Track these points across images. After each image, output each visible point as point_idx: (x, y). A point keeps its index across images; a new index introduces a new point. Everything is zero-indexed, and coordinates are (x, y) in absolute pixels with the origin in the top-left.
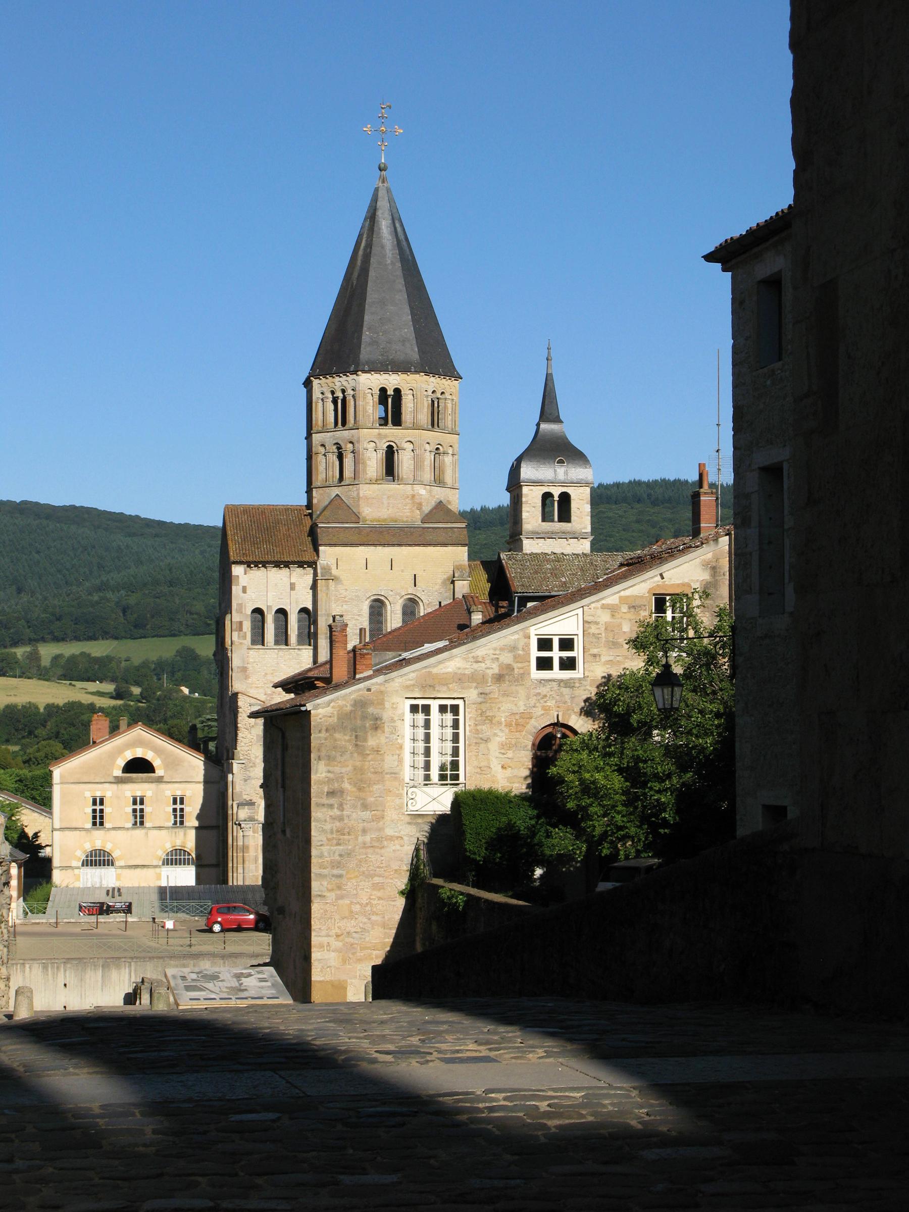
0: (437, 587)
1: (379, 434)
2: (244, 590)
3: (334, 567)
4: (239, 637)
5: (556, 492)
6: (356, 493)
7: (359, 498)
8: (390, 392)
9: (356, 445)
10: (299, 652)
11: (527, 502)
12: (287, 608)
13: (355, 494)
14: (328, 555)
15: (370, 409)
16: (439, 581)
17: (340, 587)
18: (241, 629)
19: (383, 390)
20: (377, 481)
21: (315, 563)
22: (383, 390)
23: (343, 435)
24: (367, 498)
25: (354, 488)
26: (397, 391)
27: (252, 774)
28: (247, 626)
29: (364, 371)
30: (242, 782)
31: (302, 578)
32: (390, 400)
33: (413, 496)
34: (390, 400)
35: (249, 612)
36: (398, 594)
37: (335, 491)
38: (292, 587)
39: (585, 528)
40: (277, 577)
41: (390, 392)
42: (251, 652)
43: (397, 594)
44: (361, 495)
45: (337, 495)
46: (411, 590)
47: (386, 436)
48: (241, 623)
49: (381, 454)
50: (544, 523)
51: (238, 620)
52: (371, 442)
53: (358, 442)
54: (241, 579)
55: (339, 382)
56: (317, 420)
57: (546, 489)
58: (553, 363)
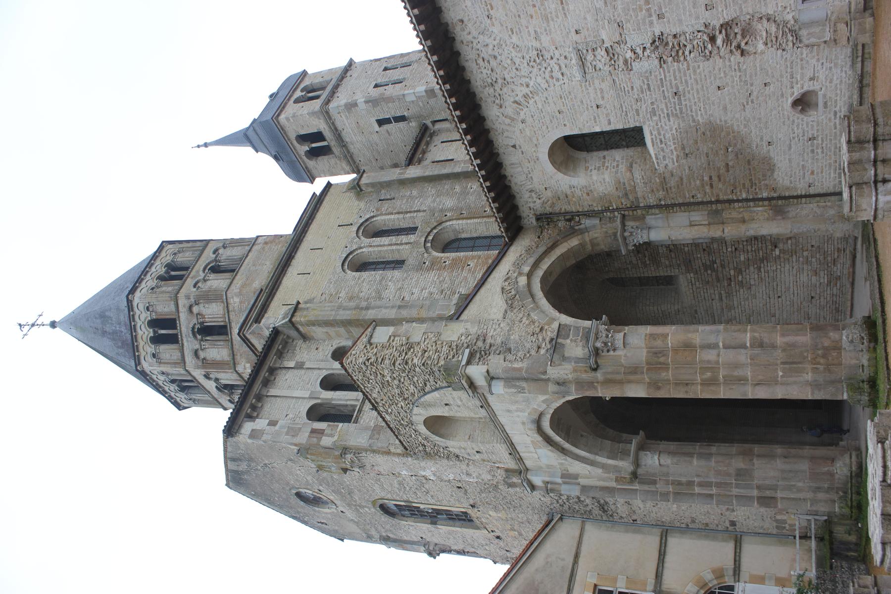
4: (332, 436)
12: (325, 373)
13: (237, 300)
18: (321, 432)
19: (161, 278)
25: (231, 301)
27: (499, 340)
28: (322, 425)
30: (510, 357)
32: (173, 273)
36: (354, 239)
38: (300, 366)
43: (352, 242)
46: (355, 228)
48: (313, 431)
49: (212, 276)
51: (307, 434)
58: (208, 141)
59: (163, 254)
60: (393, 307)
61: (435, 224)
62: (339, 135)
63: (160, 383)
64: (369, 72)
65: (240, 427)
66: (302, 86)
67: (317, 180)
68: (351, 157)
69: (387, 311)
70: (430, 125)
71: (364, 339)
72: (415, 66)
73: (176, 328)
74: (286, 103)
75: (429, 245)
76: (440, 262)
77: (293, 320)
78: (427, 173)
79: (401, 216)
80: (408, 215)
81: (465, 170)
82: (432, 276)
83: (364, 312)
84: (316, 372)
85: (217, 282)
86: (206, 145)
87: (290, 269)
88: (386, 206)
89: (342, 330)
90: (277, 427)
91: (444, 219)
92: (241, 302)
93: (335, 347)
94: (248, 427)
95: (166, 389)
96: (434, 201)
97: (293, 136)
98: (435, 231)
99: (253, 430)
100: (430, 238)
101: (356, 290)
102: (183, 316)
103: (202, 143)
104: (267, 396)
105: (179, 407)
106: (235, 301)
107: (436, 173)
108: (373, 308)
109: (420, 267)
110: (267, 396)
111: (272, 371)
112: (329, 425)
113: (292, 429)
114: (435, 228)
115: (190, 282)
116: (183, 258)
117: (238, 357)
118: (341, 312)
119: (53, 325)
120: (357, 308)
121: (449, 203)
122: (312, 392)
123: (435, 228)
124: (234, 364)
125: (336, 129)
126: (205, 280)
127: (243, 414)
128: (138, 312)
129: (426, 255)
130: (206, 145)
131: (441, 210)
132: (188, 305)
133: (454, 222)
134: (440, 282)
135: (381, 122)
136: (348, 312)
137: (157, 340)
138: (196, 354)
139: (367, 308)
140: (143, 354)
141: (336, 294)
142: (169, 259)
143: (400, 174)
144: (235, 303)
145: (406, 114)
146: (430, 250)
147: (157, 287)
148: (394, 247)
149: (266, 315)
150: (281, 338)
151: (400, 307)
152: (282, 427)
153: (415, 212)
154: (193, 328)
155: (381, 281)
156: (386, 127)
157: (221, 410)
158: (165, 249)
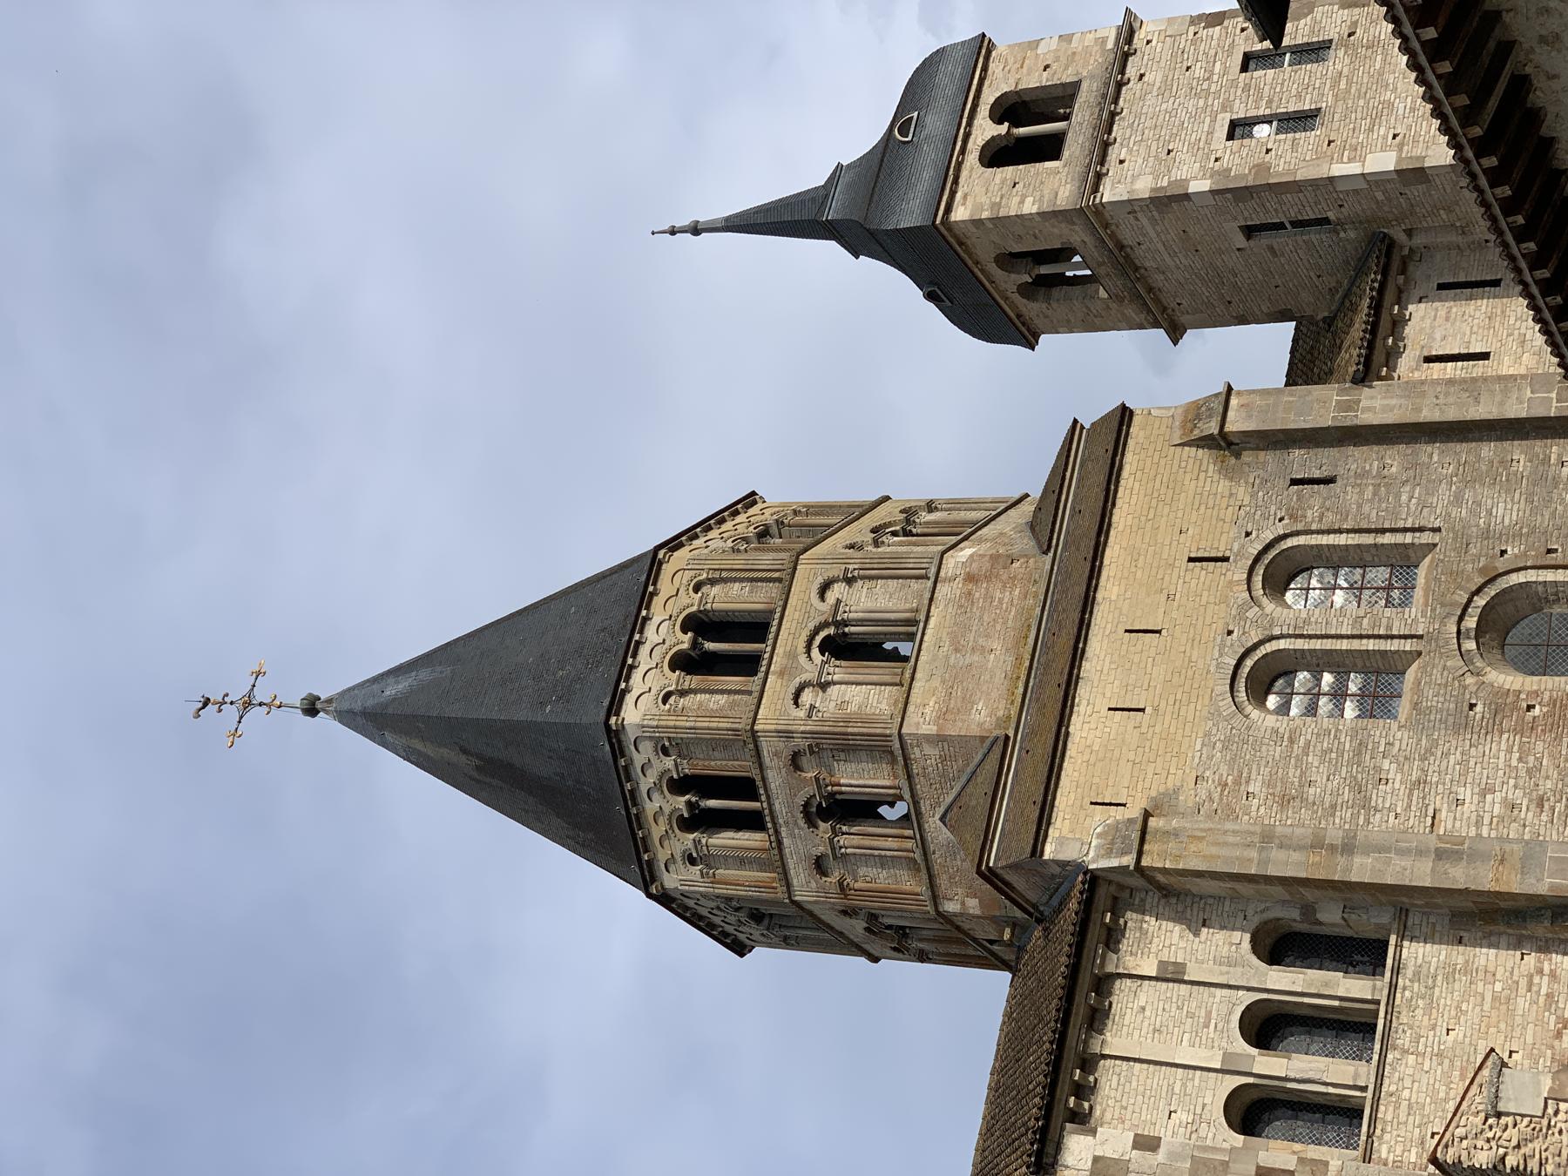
0: (1242, 493)
1: (781, 674)
2: (1147, 1143)
3: (1118, 814)
5: (985, 130)
6: (929, 750)
7: (939, 739)
8: (685, 641)
9: (803, 744)
10: (1409, 973)
11: (996, 206)
13: (932, 751)
14: (1079, 836)
15: (713, 705)
16: (1224, 485)
17: (1187, 799)
19: (681, 662)
20: (907, 687)
21: (1094, 879)
22: (681, 662)
23: (783, 793)
24: (943, 715)
25: (916, 753)
26: (698, 624)
29: (615, 705)
31: (1152, 941)
32: (710, 646)
33: (971, 578)
34: (710, 646)
35: (1239, 1140)
36: (1243, 609)
37: (933, 823)
38: (1171, 975)
39: (1104, 40)
40: (1138, 1022)
41: (685, 641)
42: (1382, 1151)
43: (1241, 616)
44: (932, 729)
45: (942, 819)
47: (792, 655)
49: (838, 670)
50: (1066, 154)
52: (795, 695)
53: (787, 734)
54: (1108, 1152)
55: (660, 806)
56: (757, 885)
57: (972, 158)
58: (703, 217)
59: (665, 586)
60: (1420, 853)
61: (1480, 580)
62: (1127, 257)
63: (704, 912)
64: (1198, 71)
65: (1058, 1147)
66: (989, 97)
67: (1044, 339)
68: (1157, 301)
69: (1406, 862)
70: (1400, 237)
71: (1479, 1100)
72: (1338, 61)
73: (756, 798)
74: (959, 165)
75: (1470, 645)
76: (1515, 707)
77: (1144, 863)
78: (1428, 414)
79: (1368, 539)
80: (1387, 539)
81: (1540, 412)
82: (1500, 751)
83: (1341, 860)
84: (1219, 992)
85: (858, 697)
86: (696, 230)
87: (1083, 692)
88: (1316, 503)
89: (1278, 891)
90: (1161, 1156)
91: (1501, 565)
92: (943, 759)
93: (1255, 921)
94: (1078, 1150)
95: (717, 920)
96: (1458, 500)
97: (985, 253)
98: (1480, 601)
99: (1096, 1159)
100: (1471, 623)
101: (1293, 774)
102: (776, 777)
103: (685, 221)
104: (1105, 1057)
105: (740, 949)
106: (926, 758)
107: (1452, 415)
108: (1369, 849)
109: (1461, 720)
110: (1105, 1057)
111: (1103, 985)
112: (1301, 1160)
113: (1205, 1162)
114: (1478, 591)
115: (777, 689)
116: (730, 598)
117: (942, 882)
118: (1276, 854)
119: (311, 708)
120: (1317, 844)
121: (1505, 511)
122: (1227, 1056)
123: (1478, 591)
124: (935, 898)
125: (1121, 247)
126: (824, 686)
127: (1059, 1113)
128: (638, 759)
129: (1470, 680)
130: (696, 230)
131: (1486, 534)
132: (787, 753)
133: (1531, 576)
134: (1529, 771)
135: (1249, 231)
136: (1296, 856)
137: (697, 821)
138: (820, 866)
139: (1348, 847)
140: (662, 855)
141: (1237, 782)
142: (691, 602)
143: (1341, 406)
144: (926, 757)
145: (1331, 215)
146: (1479, 663)
147: (683, 693)
148: (1371, 645)
149: (1053, 833)
150: (1102, 892)
151: (1440, 855)
152: (1172, 1155)
153: (1405, 530)
154: (806, 805)
155: (1358, 753)
156: (1264, 239)
157: (863, 960)
158: (667, 570)
